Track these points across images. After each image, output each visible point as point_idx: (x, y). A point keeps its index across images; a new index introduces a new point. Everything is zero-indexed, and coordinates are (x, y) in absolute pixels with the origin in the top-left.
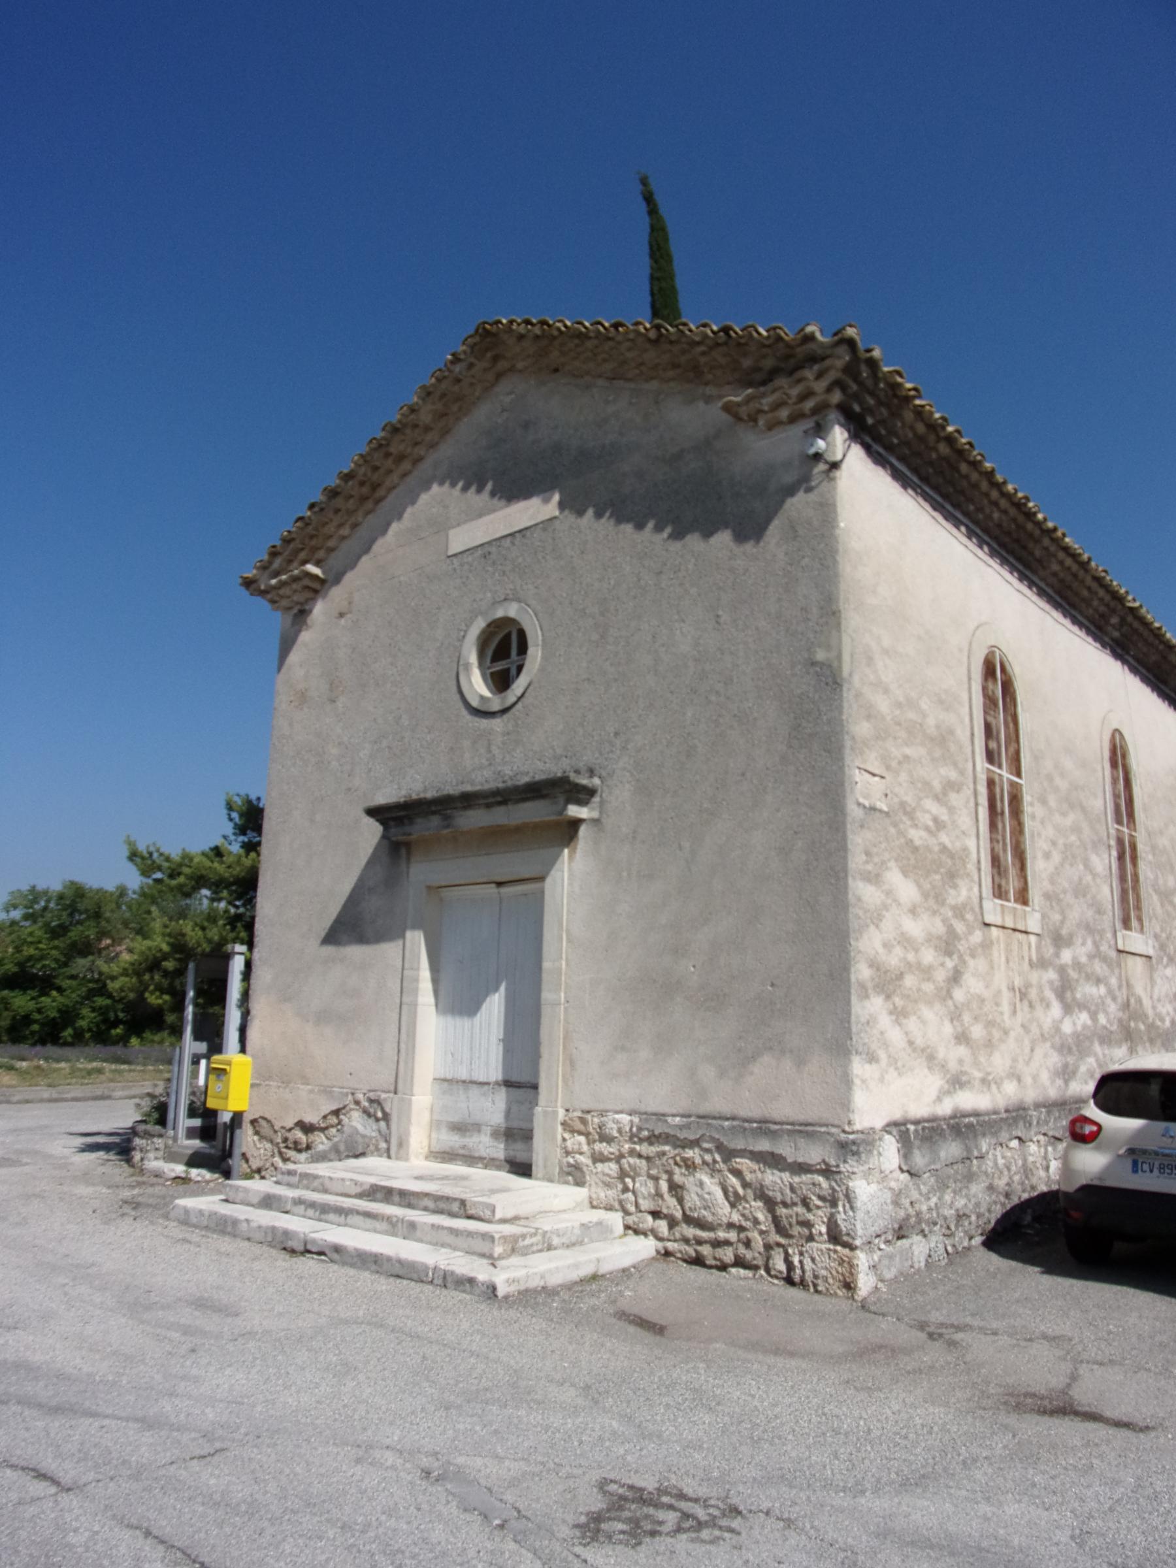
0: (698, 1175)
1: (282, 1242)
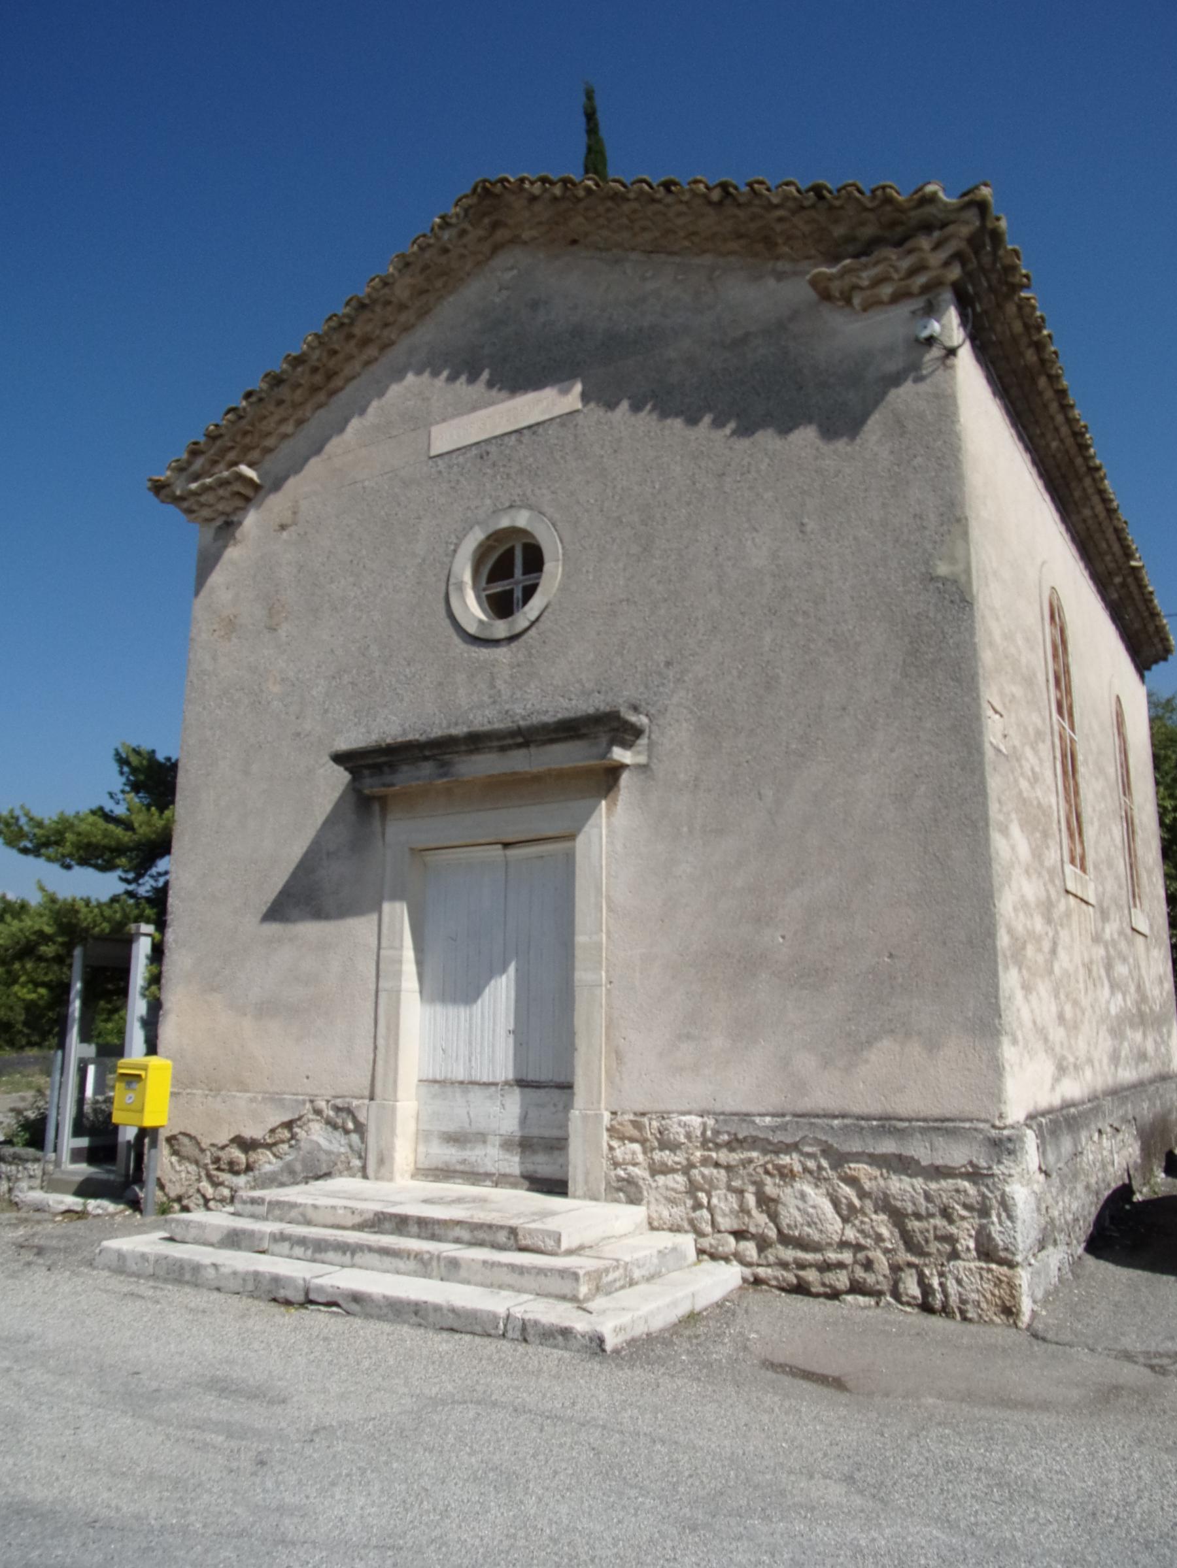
0: (797, 1185)
1: (270, 1292)
